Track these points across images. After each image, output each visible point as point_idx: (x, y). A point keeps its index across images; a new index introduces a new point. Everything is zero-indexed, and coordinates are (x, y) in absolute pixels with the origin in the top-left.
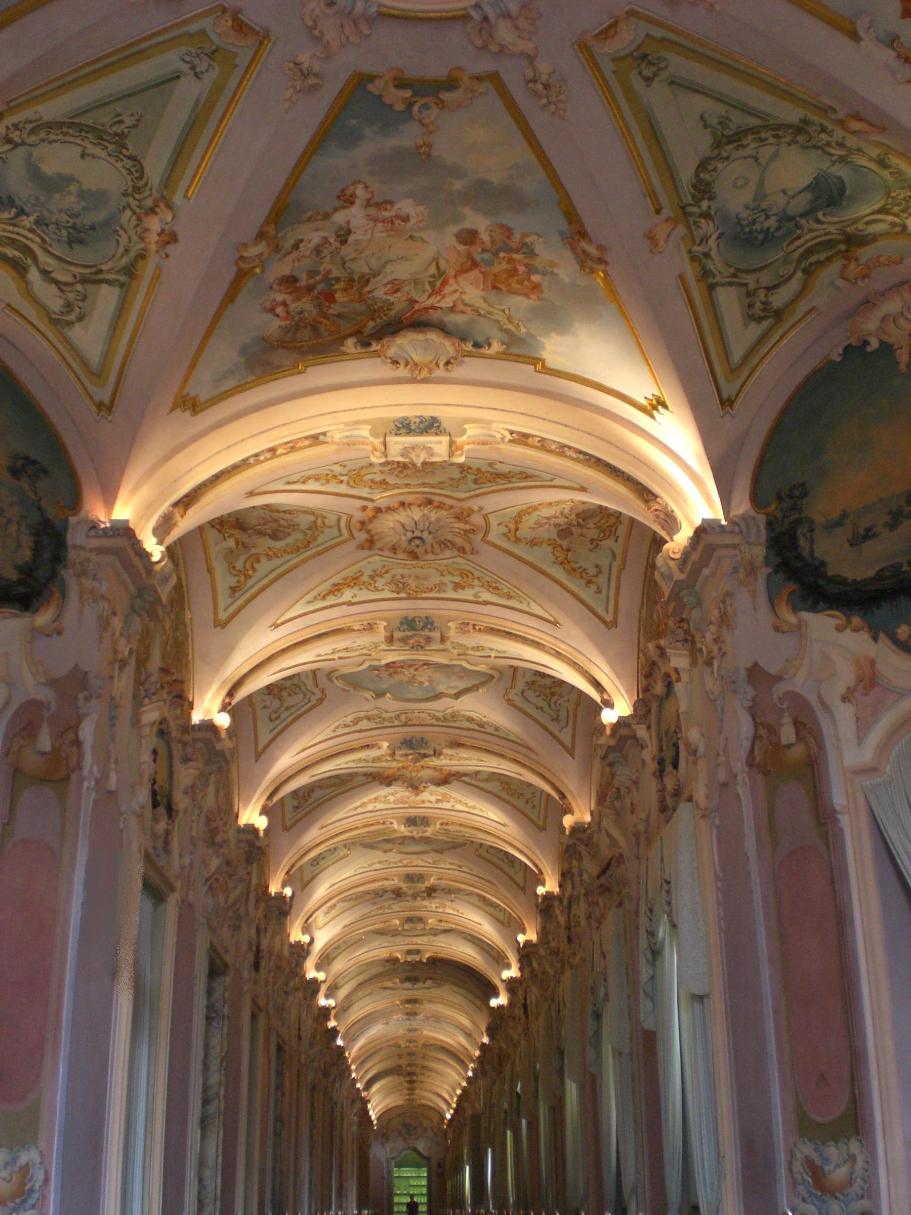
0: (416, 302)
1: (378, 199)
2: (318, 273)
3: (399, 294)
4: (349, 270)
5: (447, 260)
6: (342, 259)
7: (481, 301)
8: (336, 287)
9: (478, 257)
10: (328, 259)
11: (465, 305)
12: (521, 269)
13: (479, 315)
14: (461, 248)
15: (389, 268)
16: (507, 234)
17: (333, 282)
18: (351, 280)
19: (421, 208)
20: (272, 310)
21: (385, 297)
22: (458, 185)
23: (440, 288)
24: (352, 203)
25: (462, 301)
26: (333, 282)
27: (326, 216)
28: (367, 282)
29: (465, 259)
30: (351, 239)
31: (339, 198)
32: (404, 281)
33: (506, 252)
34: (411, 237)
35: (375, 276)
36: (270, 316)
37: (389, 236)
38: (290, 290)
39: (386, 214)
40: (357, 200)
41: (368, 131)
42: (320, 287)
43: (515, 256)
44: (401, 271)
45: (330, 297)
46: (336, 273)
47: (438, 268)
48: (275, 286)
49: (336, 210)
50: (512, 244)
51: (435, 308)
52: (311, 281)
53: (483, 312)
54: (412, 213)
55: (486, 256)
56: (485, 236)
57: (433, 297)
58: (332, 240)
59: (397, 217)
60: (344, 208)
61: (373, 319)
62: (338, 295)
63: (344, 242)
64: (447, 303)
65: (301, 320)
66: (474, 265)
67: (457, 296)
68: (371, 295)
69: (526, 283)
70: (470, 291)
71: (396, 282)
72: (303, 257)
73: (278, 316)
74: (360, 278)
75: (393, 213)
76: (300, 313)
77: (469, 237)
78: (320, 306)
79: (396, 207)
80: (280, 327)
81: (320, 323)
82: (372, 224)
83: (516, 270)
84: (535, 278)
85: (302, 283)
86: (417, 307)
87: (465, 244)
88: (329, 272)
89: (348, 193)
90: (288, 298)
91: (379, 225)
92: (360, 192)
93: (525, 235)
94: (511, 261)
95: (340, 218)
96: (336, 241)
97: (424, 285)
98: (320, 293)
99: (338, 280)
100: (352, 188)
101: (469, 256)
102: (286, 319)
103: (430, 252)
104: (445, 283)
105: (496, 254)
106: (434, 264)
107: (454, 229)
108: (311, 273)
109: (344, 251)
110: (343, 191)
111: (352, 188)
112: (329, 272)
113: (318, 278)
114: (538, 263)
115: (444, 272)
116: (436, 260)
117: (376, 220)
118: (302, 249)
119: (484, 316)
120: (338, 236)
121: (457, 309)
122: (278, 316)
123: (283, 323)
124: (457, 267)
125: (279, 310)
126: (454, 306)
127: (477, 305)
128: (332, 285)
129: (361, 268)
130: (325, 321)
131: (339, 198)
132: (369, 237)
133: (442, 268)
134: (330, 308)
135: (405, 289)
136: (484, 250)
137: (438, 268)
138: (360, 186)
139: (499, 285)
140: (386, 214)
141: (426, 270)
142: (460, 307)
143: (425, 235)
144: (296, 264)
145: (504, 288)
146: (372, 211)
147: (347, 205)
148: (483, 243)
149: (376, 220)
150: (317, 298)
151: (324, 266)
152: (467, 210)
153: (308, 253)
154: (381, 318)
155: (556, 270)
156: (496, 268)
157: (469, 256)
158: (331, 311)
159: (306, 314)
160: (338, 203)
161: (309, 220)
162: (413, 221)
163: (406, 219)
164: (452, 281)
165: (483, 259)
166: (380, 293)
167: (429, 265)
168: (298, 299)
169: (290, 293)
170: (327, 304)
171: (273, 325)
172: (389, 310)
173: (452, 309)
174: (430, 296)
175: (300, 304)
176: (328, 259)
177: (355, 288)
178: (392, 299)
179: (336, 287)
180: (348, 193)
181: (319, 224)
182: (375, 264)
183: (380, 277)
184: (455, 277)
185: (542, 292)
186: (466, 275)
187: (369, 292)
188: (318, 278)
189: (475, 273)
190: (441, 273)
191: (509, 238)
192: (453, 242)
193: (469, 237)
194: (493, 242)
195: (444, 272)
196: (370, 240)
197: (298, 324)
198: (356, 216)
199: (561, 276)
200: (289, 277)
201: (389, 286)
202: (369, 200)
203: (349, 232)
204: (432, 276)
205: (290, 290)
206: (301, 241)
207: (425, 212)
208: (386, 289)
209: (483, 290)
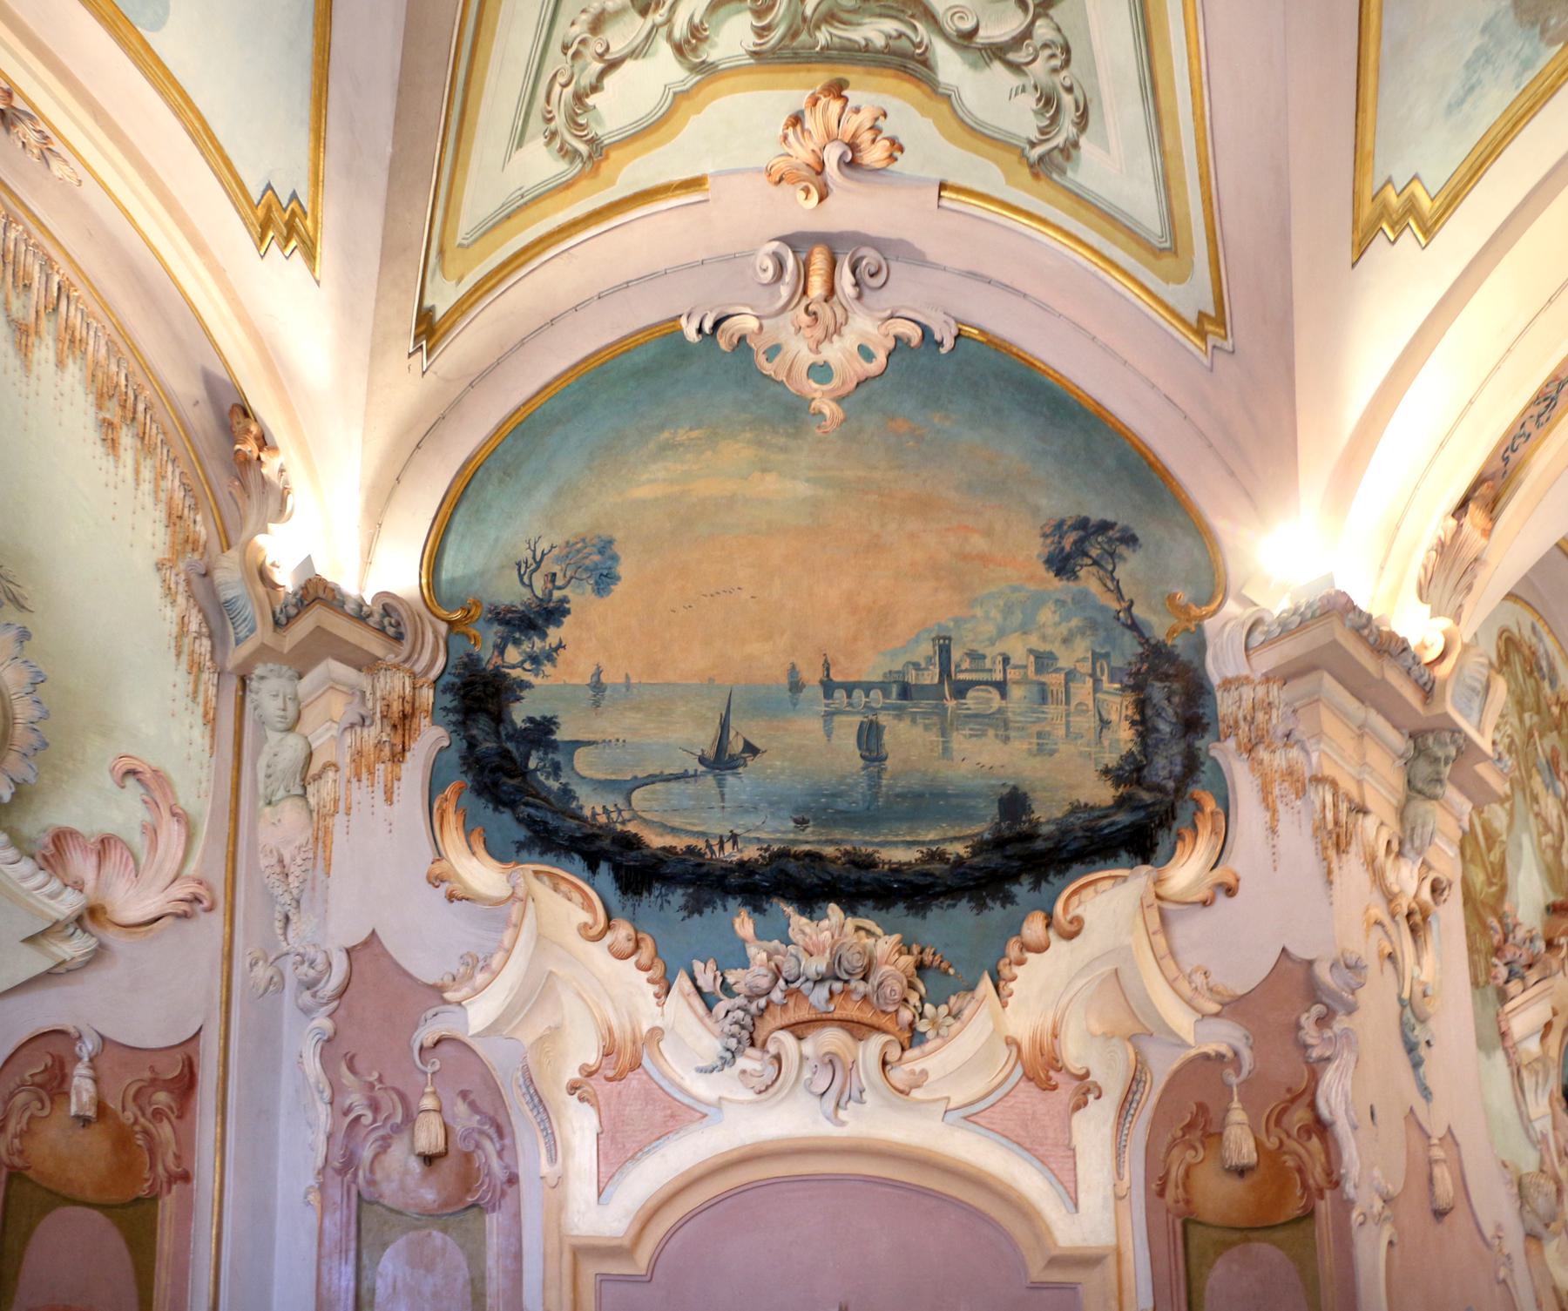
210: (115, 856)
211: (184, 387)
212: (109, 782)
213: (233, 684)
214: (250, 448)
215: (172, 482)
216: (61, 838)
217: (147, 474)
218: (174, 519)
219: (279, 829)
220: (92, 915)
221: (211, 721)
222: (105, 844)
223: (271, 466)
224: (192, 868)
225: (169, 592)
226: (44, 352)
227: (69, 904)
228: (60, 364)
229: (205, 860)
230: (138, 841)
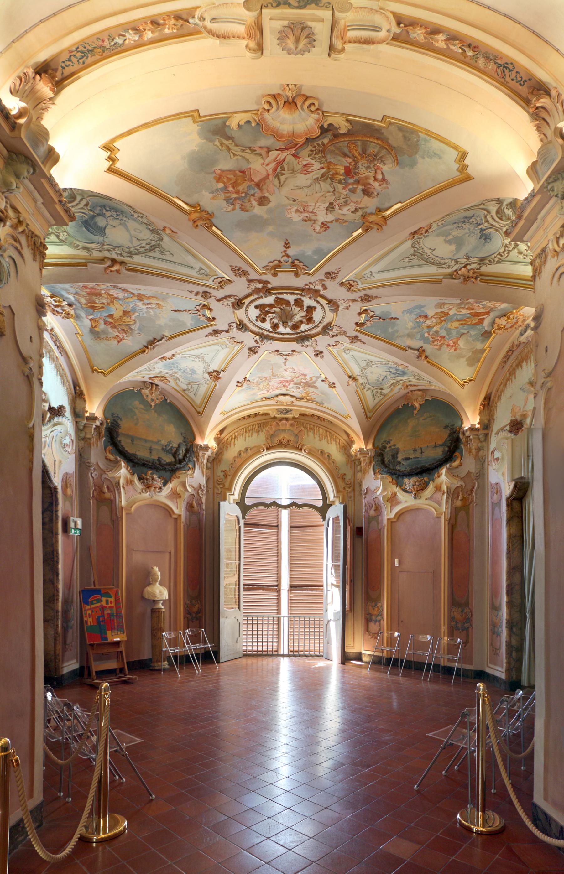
0: (294, 155)
1: (309, 222)
2: (349, 190)
3: (305, 163)
4: (332, 186)
5: (274, 185)
6: (335, 195)
7: (250, 160)
8: (342, 177)
9: (257, 190)
10: (342, 196)
11: (260, 155)
12: (231, 189)
13: (250, 148)
14: (267, 195)
15: (309, 182)
16: (243, 207)
17: (343, 181)
18: (332, 179)
19: (289, 216)
20: (383, 180)
21: (313, 162)
22: (270, 228)
23: (278, 166)
24: (322, 223)
25: (262, 157)
26: (343, 181)
27: (337, 220)
28: (322, 176)
29: (264, 187)
30: (327, 205)
31: (328, 227)
32: (300, 173)
33: (241, 197)
34: (294, 201)
35: (317, 178)
36: (387, 177)
37: (307, 203)
38: (369, 186)
39: (306, 215)
40: (320, 224)
41: (310, 253)
42: (351, 181)
43: (235, 196)
44: (302, 180)
45: (348, 172)
46: (340, 186)
47: (279, 180)
48: (376, 194)
49: (332, 222)
50: (240, 202)
51: (281, 150)
52: (355, 186)
53: (248, 151)
54: (293, 214)
55: (252, 192)
56: (255, 203)
57: (282, 159)
58: (337, 207)
59: (302, 212)
60: (326, 222)
61: (324, 145)
62: (342, 171)
63: (331, 204)
64: (273, 154)
65: (370, 162)
66: (258, 185)
67: (267, 161)
68: (322, 165)
69: (225, 180)
70: (259, 167)
71: (305, 172)
72: (354, 203)
73: (382, 173)
74: (327, 179)
75: (304, 215)
76: (369, 167)
77: (263, 201)
78: (356, 167)
79: (301, 218)
80: (385, 164)
81: (359, 154)
82: (315, 211)
83: (233, 187)
84: (221, 185)
85: (361, 187)
86: (293, 151)
87: (264, 197)
88: (344, 189)
89: (323, 229)
90: (371, 181)
91: (311, 210)
92: (318, 228)
93: (233, 209)
94: (237, 192)
95: (330, 217)
96: (335, 206)
97: (288, 168)
98: (353, 177)
99: (340, 182)
100: (321, 230)
101: (261, 189)
102: (379, 168)
103: (285, 191)
104: (275, 170)
105: (247, 194)
106: (282, 183)
107: (271, 205)
108: (353, 191)
109: (331, 198)
110: (325, 230)
111: (321, 230)
112: (344, 189)
113: (351, 187)
114: (223, 196)
115: (275, 177)
116: (281, 186)
117: (312, 212)
118: (354, 207)
119: (246, 148)
120: (333, 208)
121: (266, 150)
122: (382, 173)
123: (381, 165)
124: (267, 181)
125: (379, 177)
126: (268, 152)
127: (252, 155)
128: (344, 179)
129: (326, 186)
130: (356, 154)
131: (328, 227)
132: (318, 204)
133: (276, 180)
134: (350, 164)
135: (300, 167)
136: (253, 195)
137: (279, 180)
138: (317, 231)
139: (241, 174)
140: (306, 215)
141: (286, 178)
142: (263, 152)
143: (287, 202)
144: (359, 200)
145: (238, 172)
146: (313, 217)
147: (325, 223)
148: (255, 199)
149: (312, 212)
150: (355, 173)
151: (345, 193)
152: (265, 216)
153: (352, 204)
154: (318, 144)
155: (211, 195)
156: (245, 185)
157: (261, 189)
158: (350, 160)
159: (366, 165)
160: (329, 225)
161: (346, 221)
162: (293, 210)
163: (297, 211)
164: (270, 172)
165: (254, 189)
166: (317, 166)
167: (284, 182)
168: (367, 178)
169: (370, 184)
170: (351, 167)
171: (387, 168)
172: (312, 151)
173: (269, 150)
174: (284, 159)
175: (367, 174)
176: (342, 196)
177: (331, 173)
178: (309, 160)
179: (342, 177)
180: (323, 229)
181: (341, 217)
182: (317, 186)
183: (315, 177)
184: (268, 175)
185: (215, 178)
186: (263, 177)
187: (323, 168)
188: (351, 187)
189: (257, 179)
190: (277, 177)
191: (242, 205)
192: (271, 198)
193: (263, 201)
194: (249, 201)
195: (275, 177)
196: (317, 202)
197: (374, 158)
198: (322, 217)
199: (207, 193)
200: (366, 195)
201: (310, 170)
202: (314, 223)
203: (327, 209)
204: (283, 174)
205: (369, 186)
206: (352, 212)
207: (286, 214)
208: (312, 168)
209: (250, 168)
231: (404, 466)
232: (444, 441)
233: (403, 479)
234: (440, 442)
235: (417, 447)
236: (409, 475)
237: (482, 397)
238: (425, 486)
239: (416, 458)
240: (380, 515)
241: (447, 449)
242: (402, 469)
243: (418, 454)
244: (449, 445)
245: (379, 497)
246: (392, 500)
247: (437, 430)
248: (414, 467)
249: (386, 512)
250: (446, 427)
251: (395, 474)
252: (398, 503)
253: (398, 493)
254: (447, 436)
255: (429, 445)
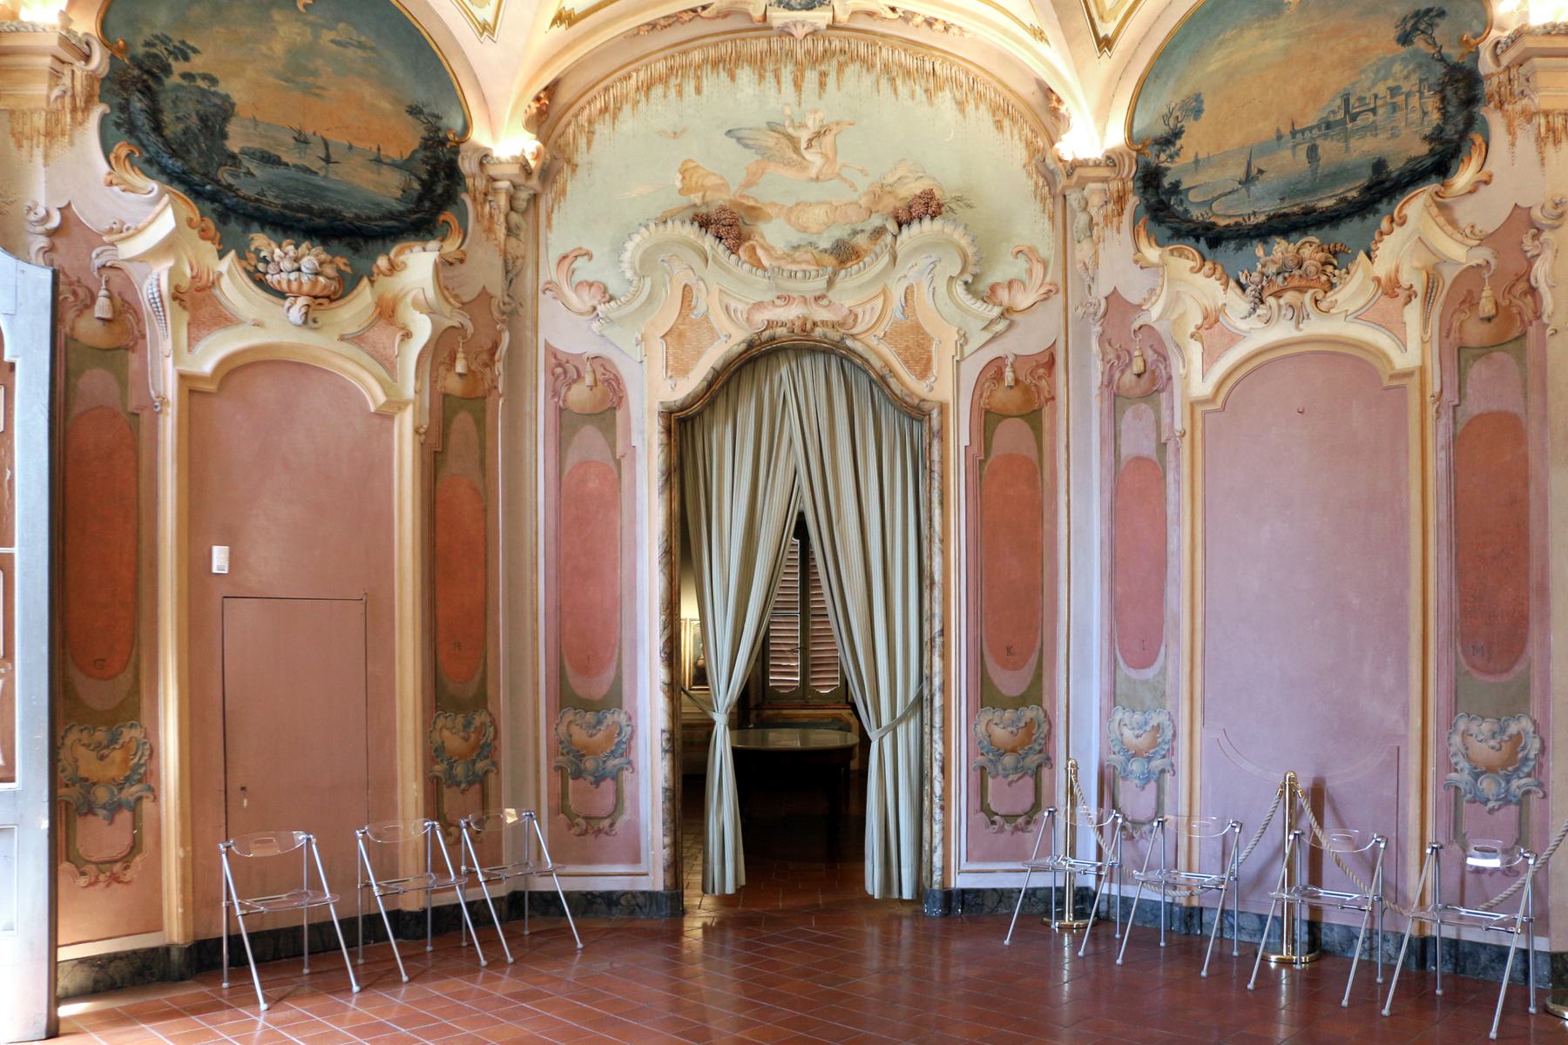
210: (1015, 286)
211: (1028, 91)
212: (1011, 258)
213: (1060, 199)
214: (1055, 104)
215: (1027, 131)
216: (993, 288)
217: (1016, 132)
218: (1028, 144)
219: (1082, 251)
220: (1007, 312)
221: (1052, 218)
222: (1010, 284)
223: (1063, 109)
224: (1048, 279)
225: (1029, 175)
226: (970, 107)
227: (996, 311)
228: (977, 107)
229: (1054, 274)
230: (1025, 277)
231: (251, 182)
232: (406, 155)
233: (247, 229)
234: (393, 152)
235: (309, 132)
236: (286, 224)
237: (547, 79)
238: (345, 286)
239: (307, 170)
240: (133, 349)
241: (416, 185)
242: (248, 190)
243: (312, 159)
244: (425, 176)
245: (134, 271)
246: (197, 303)
247: (385, 105)
248: (297, 201)
249: (167, 345)
250: (414, 111)
251: (213, 198)
252: (223, 319)
253: (225, 283)
254: (416, 144)
255: (356, 144)
